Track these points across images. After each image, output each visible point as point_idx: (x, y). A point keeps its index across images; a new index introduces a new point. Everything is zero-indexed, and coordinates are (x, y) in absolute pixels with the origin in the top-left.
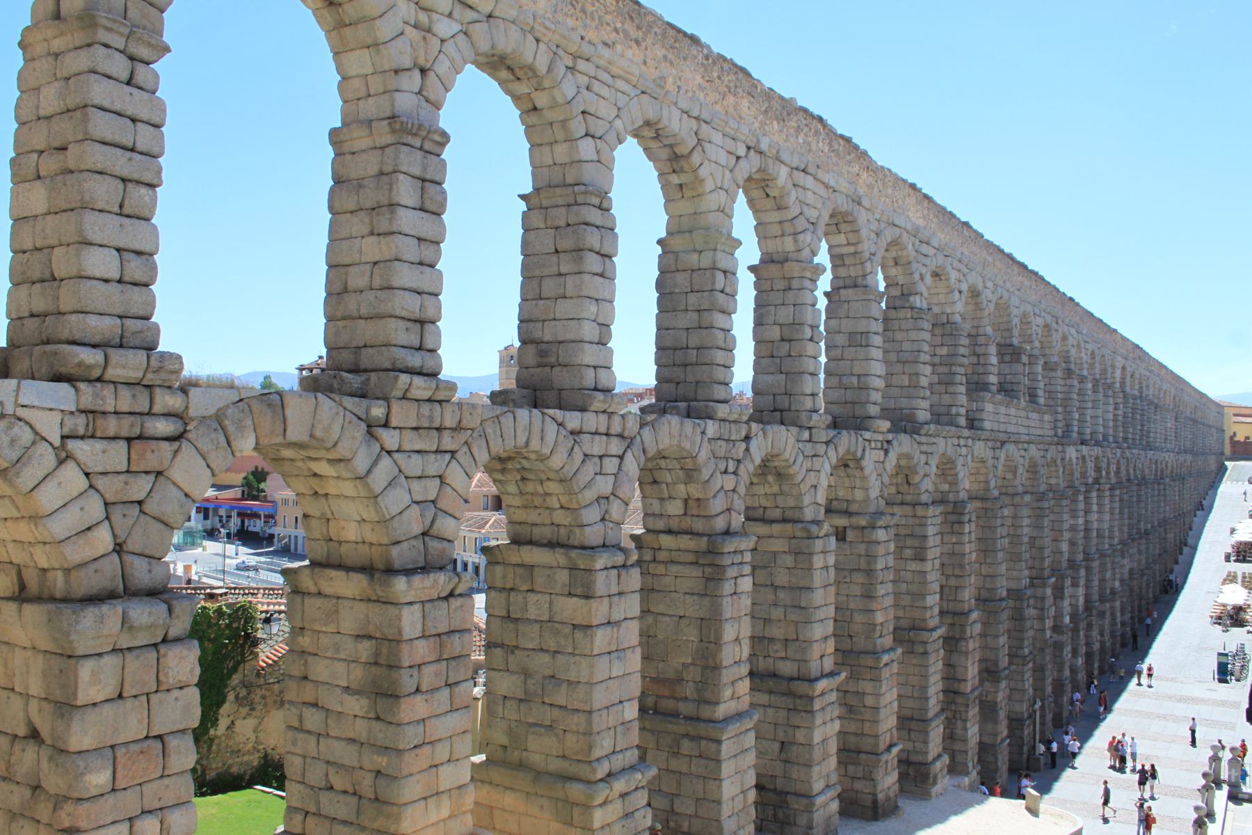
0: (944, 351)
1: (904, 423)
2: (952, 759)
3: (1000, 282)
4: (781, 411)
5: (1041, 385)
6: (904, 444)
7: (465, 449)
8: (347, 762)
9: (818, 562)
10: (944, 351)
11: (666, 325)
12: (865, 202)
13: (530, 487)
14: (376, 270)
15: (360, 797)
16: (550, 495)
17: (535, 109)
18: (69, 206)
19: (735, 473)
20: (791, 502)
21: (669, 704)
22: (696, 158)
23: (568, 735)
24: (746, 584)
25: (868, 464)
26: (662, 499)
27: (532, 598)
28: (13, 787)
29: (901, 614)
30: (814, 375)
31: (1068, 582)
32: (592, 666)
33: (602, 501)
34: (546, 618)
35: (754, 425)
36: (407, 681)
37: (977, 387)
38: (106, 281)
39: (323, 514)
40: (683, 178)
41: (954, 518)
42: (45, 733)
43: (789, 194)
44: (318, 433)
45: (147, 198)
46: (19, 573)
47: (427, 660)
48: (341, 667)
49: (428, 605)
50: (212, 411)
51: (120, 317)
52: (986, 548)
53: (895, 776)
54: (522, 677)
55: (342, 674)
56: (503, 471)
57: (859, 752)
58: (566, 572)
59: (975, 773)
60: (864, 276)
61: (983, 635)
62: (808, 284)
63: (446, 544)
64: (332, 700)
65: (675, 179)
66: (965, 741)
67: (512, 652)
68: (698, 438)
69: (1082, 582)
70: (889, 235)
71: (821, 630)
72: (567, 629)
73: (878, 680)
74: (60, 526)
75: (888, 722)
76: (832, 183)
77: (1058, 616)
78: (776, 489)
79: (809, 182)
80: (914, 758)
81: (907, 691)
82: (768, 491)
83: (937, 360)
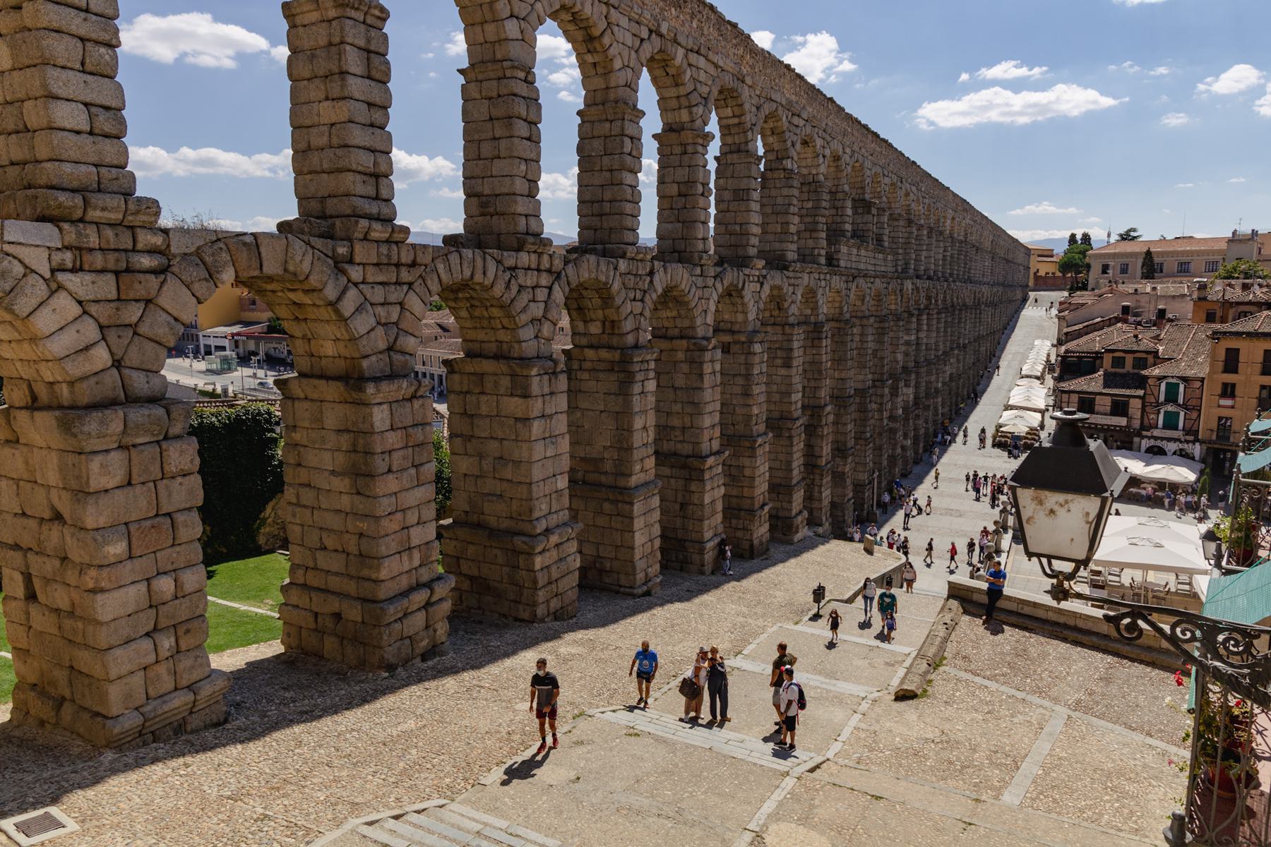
0: (810, 205)
1: (777, 262)
2: (811, 513)
3: (856, 148)
4: (679, 252)
5: (887, 232)
6: (776, 278)
7: (420, 281)
8: (335, 528)
9: (707, 368)
10: (810, 205)
11: (585, 183)
12: (749, 81)
13: (477, 313)
14: (334, 130)
18: (31, 62)
19: (642, 301)
20: (686, 323)
21: (592, 477)
22: (606, 40)
23: (514, 502)
24: (651, 385)
25: (748, 294)
26: (585, 322)
27: (484, 398)
28: (45, 559)
29: (772, 407)
30: (705, 223)
31: (902, 384)
32: (530, 449)
34: (494, 413)
35: (656, 263)
36: (380, 464)
37: (835, 235)
38: (78, 132)
40: (597, 58)
41: (815, 335)
42: (66, 516)
43: (684, 72)
44: (291, 268)
45: (107, 57)
46: (30, 386)
47: (396, 447)
48: (327, 456)
49: (394, 405)
50: (193, 249)
51: (96, 166)
52: (839, 361)
53: (767, 526)
55: (327, 460)
56: (456, 300)
57: (740, 510)
58: (508, 378)
59: (827, 525)
60: (747, 143)
61: (836, 423)
62: (700, 149)
63: (408, 357)
64: (322, 481)
65: (590, 58)
66: (820, 500)
68: (612, 273)
69: (913, 383)
70: (767, 108)
71: (710, 420)
72: (512, 422)
73: (753, 456)
74: (58, 346)
75: (761, 488)
76: (721, 64)
77: (894, 408)
78: (674, 313)
79: (702, 62)
80: (781, 514)
81: (777, 465)
82: (669, 314)
83: (804, 212)
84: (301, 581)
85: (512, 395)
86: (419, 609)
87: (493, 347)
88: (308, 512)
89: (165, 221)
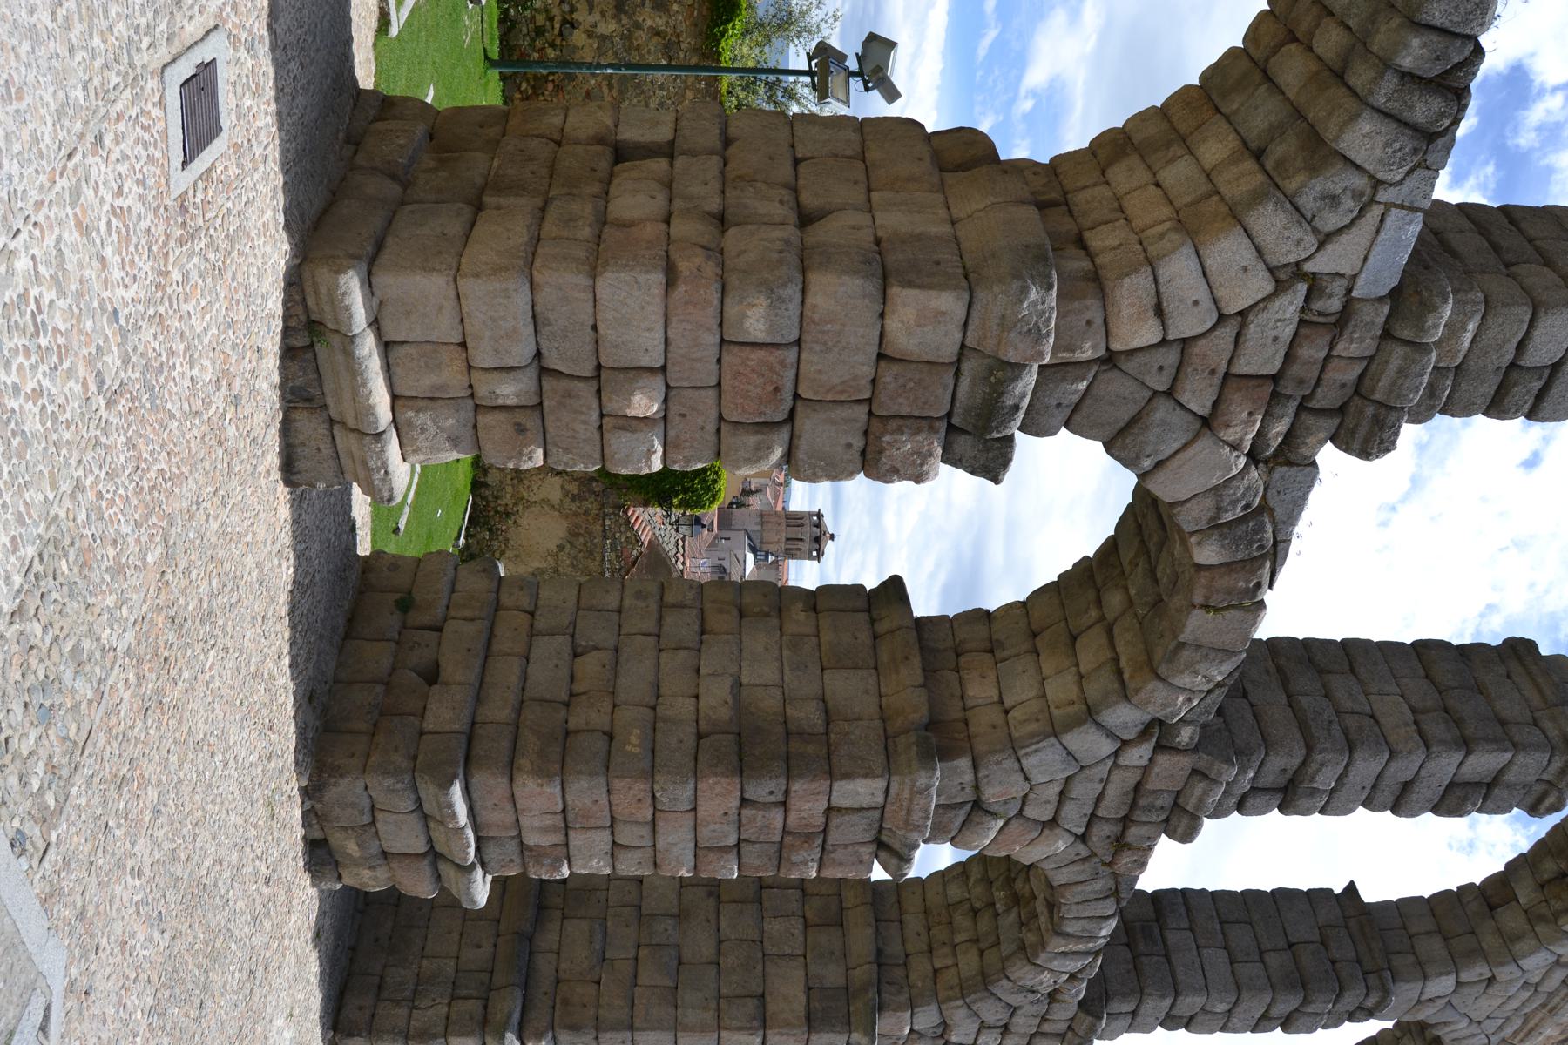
8: (622, 681)
15: (567, 705)
16: (955, 955)
17: (1492, 908)
23: (591, 990)
27: (796, 926)
33: (939, 1031)
34: (769, 949)
36: (761, 790)
38: (1521, 347)
39: (1002, 645)
47: (793, 818)
48: (769, 673)
54: (675, 911)
55: (761, 672)
58: (841, 982)
67: (710, 894)
84: (506, 600)
85: (809, 989)
86: (430, 840)
87: (894, 948)
88: (650, 625)
89: (1329, 457)
